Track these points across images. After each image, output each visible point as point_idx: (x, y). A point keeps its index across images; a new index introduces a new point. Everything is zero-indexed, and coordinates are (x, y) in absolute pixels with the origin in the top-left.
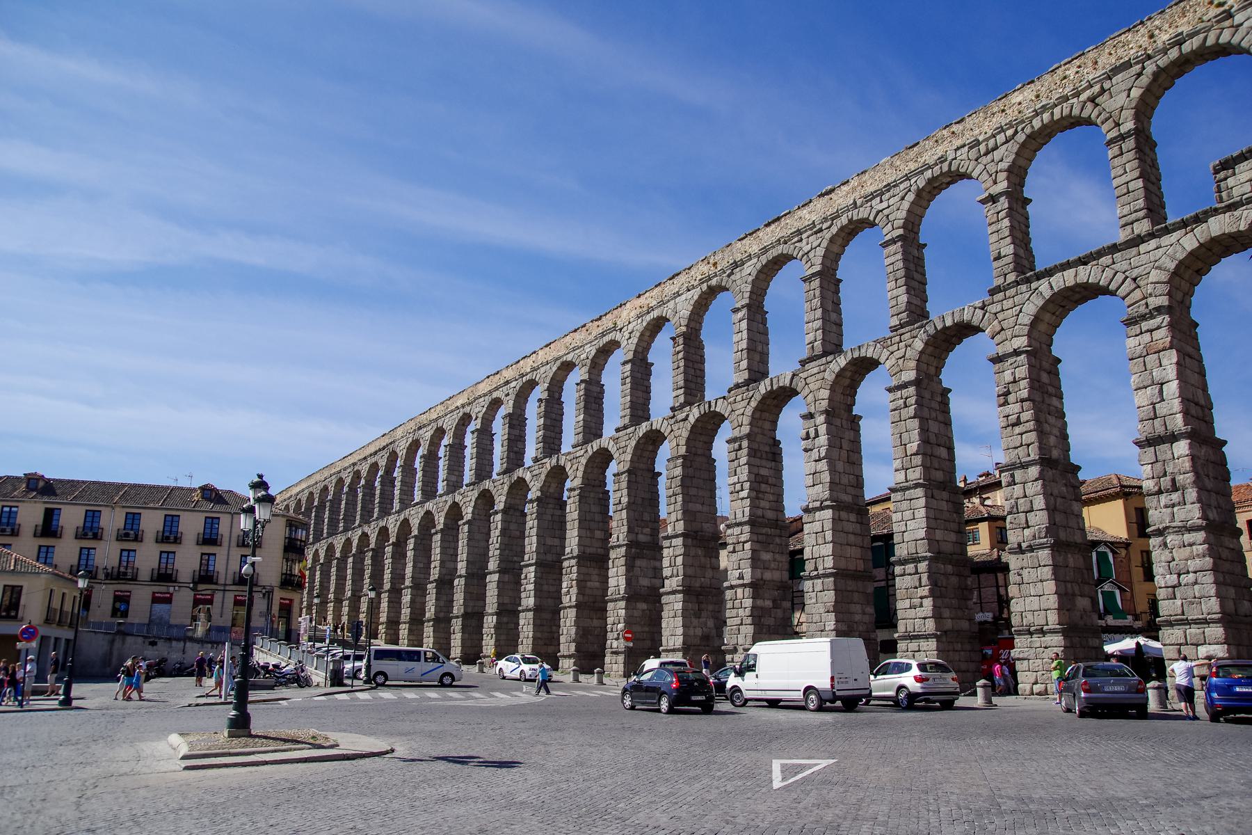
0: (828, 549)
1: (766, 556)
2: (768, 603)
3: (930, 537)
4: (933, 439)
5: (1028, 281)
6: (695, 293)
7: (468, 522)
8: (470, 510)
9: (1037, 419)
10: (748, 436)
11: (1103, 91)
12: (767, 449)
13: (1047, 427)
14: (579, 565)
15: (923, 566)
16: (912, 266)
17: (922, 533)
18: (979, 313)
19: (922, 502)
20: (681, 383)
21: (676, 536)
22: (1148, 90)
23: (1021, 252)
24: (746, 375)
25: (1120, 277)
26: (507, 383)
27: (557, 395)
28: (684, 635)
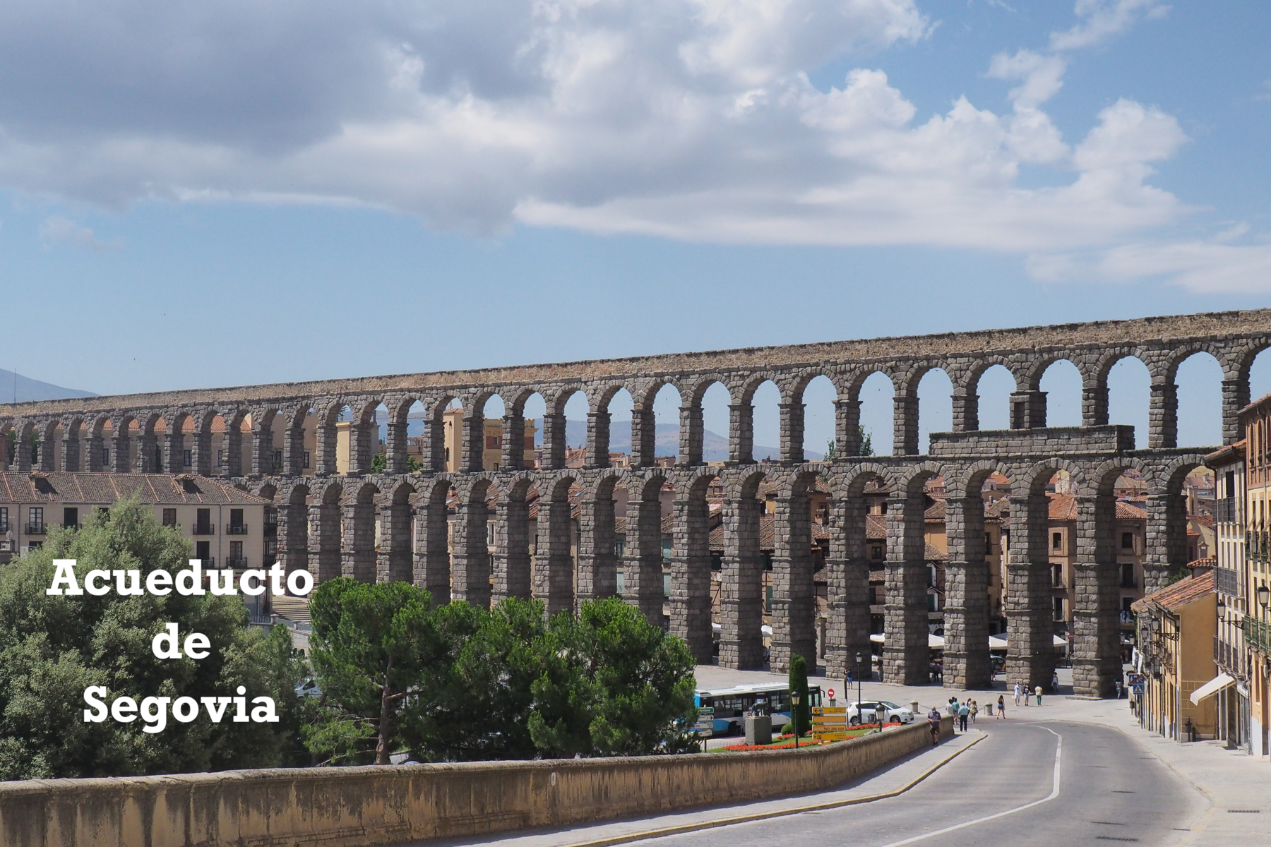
0: (736, 587)
1: (696, 581)
2: (697, 612)
3: (791, 591)
5: (851, 461)
6: (651, 382)
7: (427, 507)
8: (428, 494)
9: (847, 538)
10: (687, 503)
13: (852, 542)
14: (550, 564)
15: (786, 606)
17: (787, 588)
19: (788, 570)
20: (639, 448)
21: (634, 559)
22: (914, 375)
23: (852, 438)
24: (688, 459)
26: (466, 387)
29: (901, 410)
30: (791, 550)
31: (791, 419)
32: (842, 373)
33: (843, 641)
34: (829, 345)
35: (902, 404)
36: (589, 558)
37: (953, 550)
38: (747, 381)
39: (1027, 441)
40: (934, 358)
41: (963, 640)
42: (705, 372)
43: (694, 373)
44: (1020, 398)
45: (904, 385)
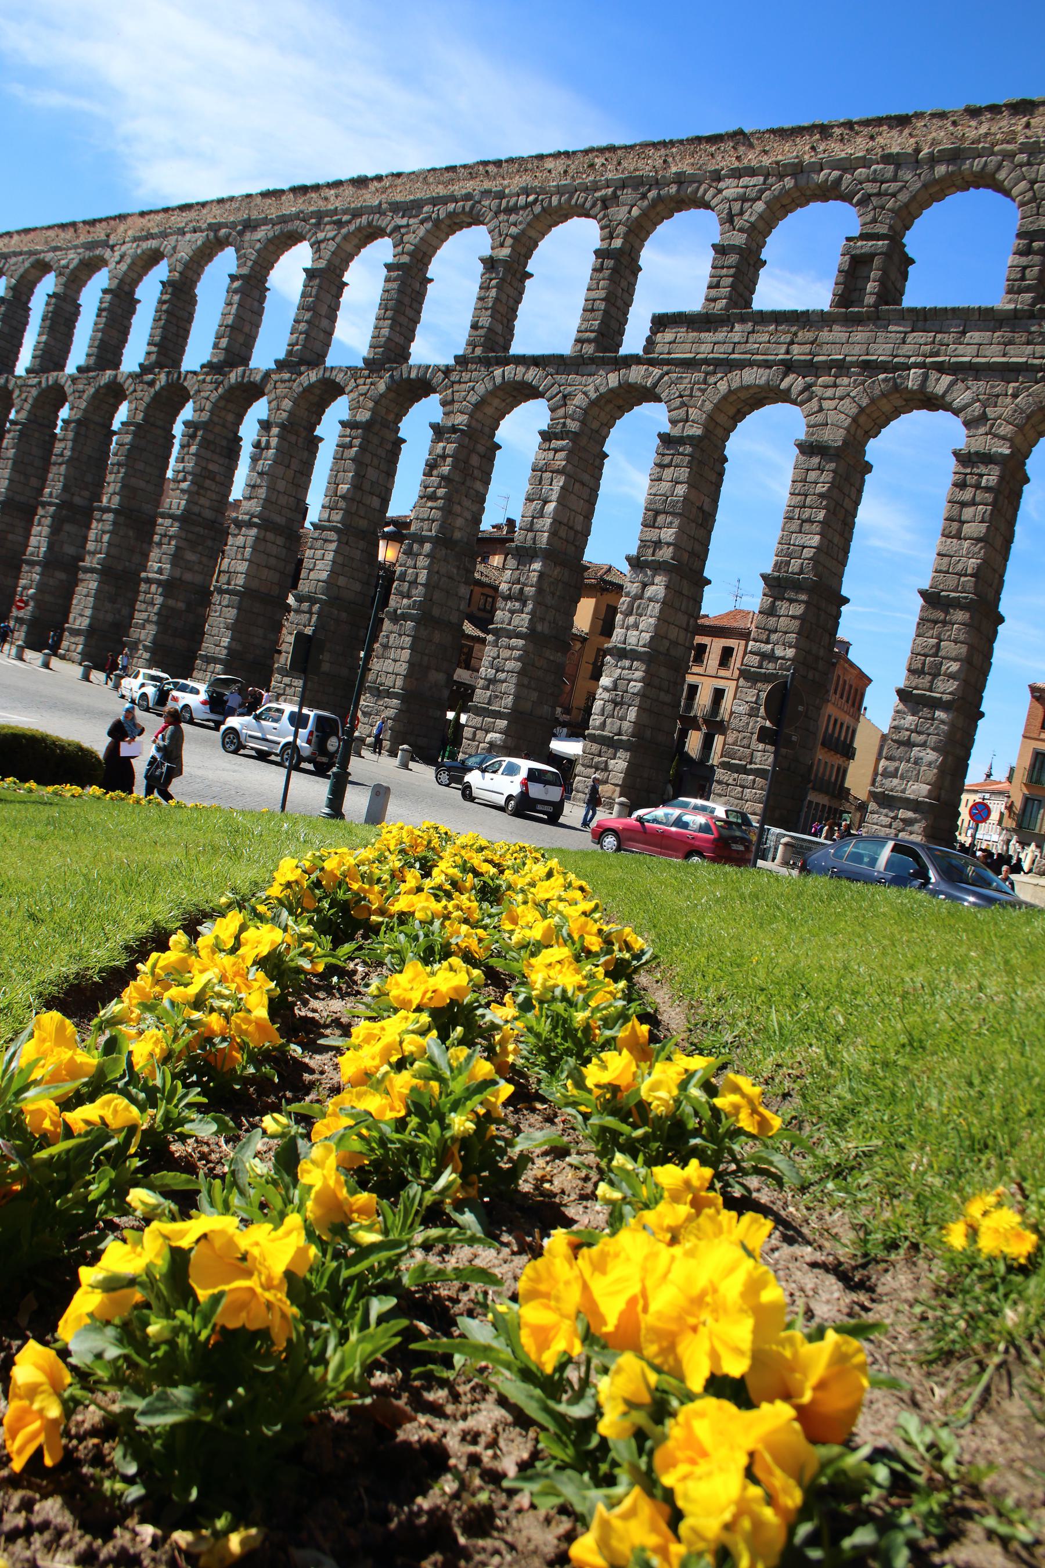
0: (243, 567)
1: (190, 556)
2: (181, 605)
3: (330, 583)
4: (367, 486)
6: (199, 238)
9: (448, 498)
11: (615, 196)
12: (224, 443)
13: (457, 509)
15: (316, 608)
16: (407, 300)
17: (324, 575)
18: (440, 375)
19: (333, 546)
20: (157, 339)
23: (499, 328)
25: (555, 389)
27: (24, 298)
28: (92, 618)
29: (607, 273)
30: (347, 512)
31: (400, 291)
32: (510, 210)
33: (399, 683)
34: (498, 163)
35: (609, 263)
36: (50, 504)
37: (652, 535)
38: (344, 231)
39: (860, 335)
40: (694, 179)
41: (632, 714)
42: (284, 219)
43: (265, 221)
44: (866, 246)
45: (621, 229)
